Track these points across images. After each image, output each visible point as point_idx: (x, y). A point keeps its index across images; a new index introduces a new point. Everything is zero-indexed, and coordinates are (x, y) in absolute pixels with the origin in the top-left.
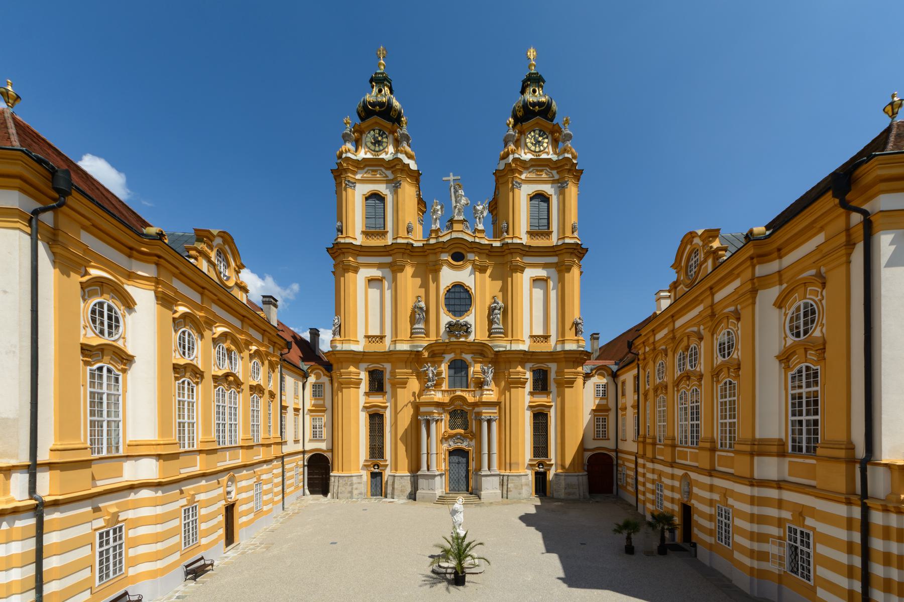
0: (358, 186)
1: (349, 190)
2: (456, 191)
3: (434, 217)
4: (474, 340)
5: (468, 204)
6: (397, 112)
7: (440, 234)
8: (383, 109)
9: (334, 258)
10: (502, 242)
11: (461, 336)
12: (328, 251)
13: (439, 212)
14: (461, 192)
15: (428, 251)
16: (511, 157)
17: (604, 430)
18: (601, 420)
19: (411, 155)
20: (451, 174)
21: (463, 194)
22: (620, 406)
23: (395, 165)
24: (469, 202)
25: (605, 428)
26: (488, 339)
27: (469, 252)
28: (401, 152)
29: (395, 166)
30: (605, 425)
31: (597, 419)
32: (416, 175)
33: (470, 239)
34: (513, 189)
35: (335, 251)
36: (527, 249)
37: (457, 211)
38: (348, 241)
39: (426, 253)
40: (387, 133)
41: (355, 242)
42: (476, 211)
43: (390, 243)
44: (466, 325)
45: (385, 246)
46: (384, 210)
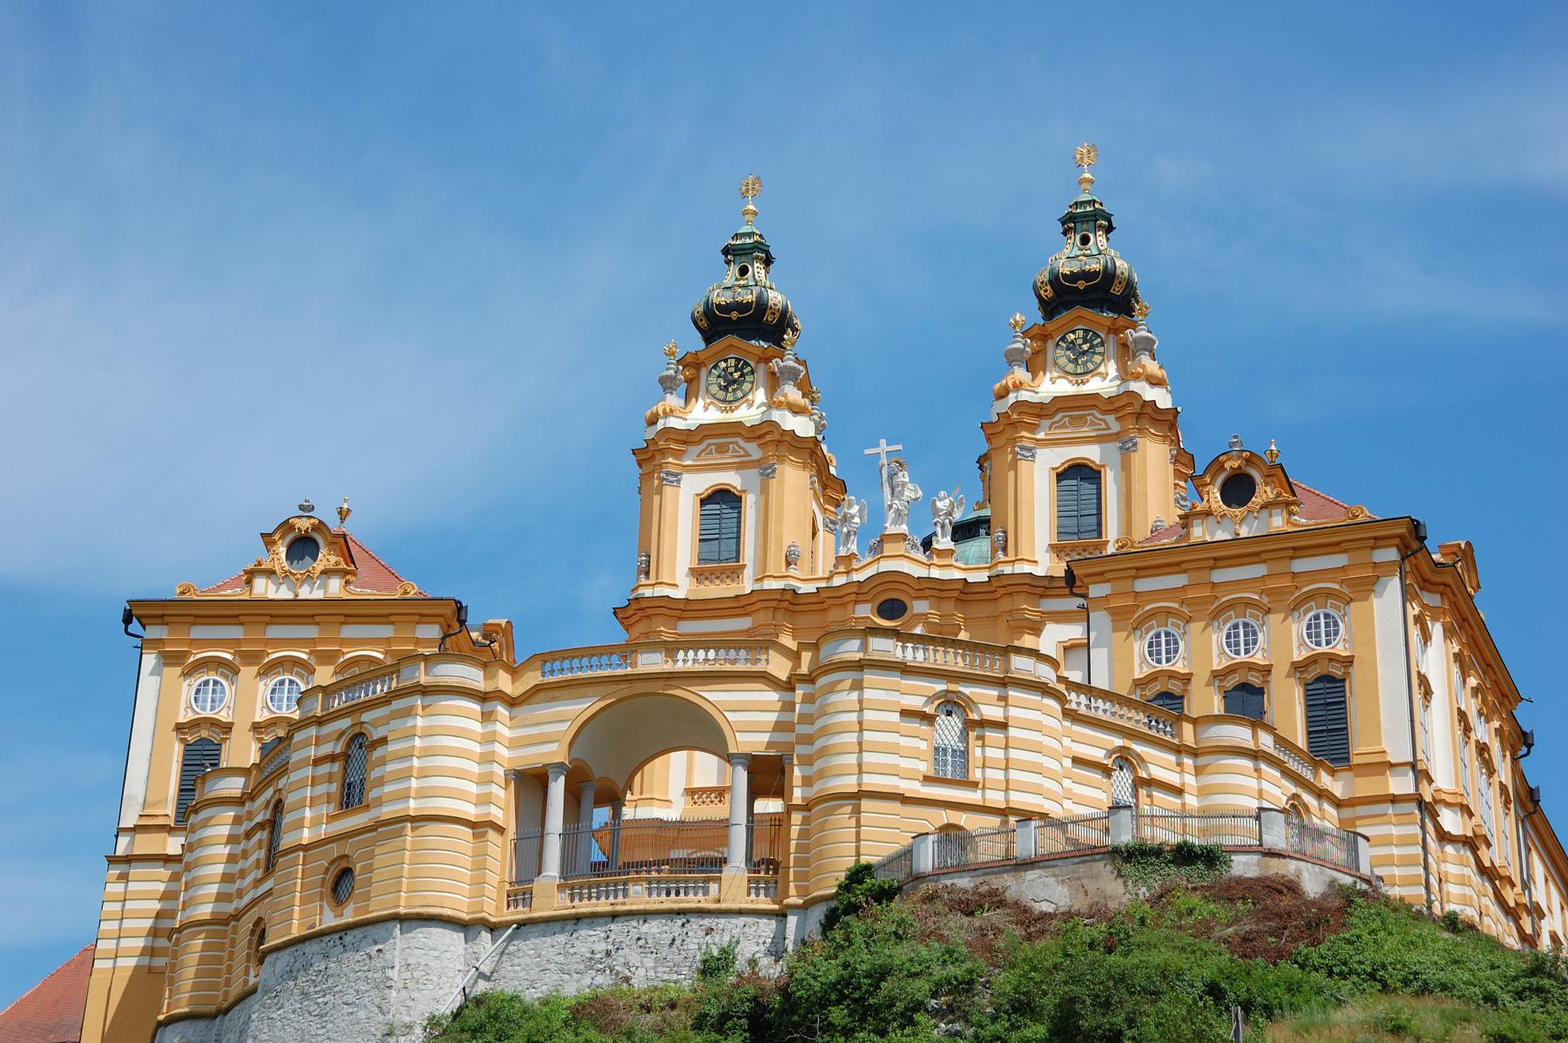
0: (687, 478)
1: (668, 490)
2: (891, 476)
3: (845, 530)
5: (916, 499)
6: (777, 315)
7: (855, 565)
10: (993, 572)
12: (615, 613)
13: (857, 520)
14: (904, 477)
15: (829, 602)
16: (1012, 398)
19: (799, 406)
20: (883, 442)
21: (907, 480)
23: (765, 433)
24: (920, 493)
27: (916, 598)
28: (779, 406)
29: (764, 435)
32: (811, 445)
33: (918, 571)
34: (1014, 465)
35: (632, 612)
36: (1046, 583)
37: (891, 514)
38: (660, 591)
40: (752, 364)
42: (936, 511)
43: (748, 591)
46: (739, 522)
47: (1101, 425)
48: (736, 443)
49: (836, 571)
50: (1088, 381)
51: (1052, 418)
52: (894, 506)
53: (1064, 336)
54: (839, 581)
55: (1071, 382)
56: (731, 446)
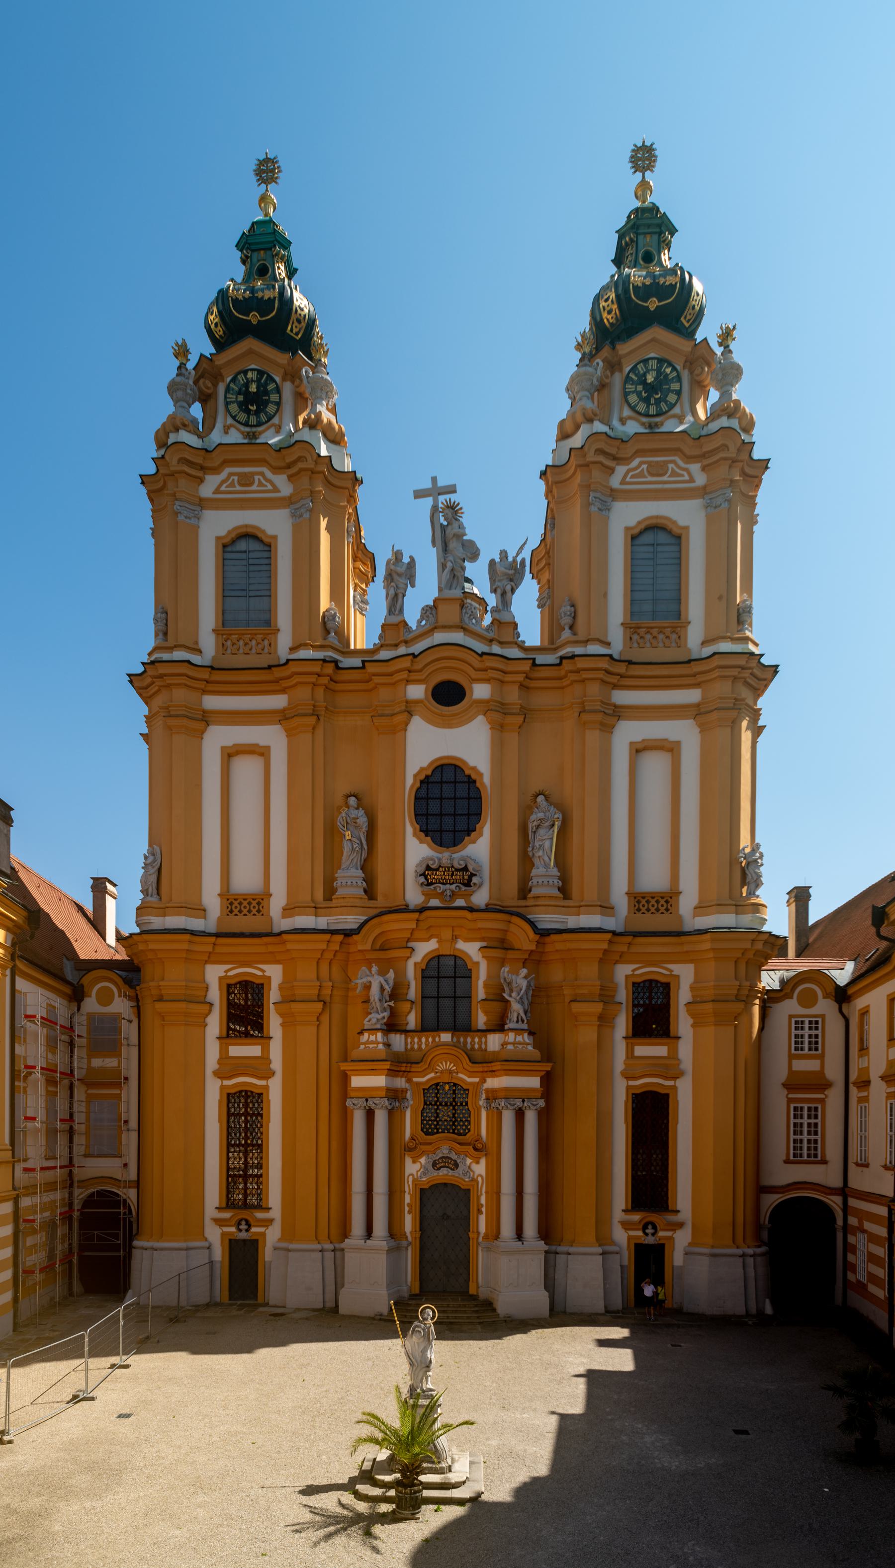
4: (487, 905)
8: (264, 319)
9: (147, 700)
11: (454, 895)
15: (376, 680)
17: (813, 1137)
18: (805, 1113)
22: (853, 1077)
25: (816, 1133)
26: (522, 903)
29: (294, 463)
30: (816, 1125)
31: (795, 1109)
32: (349, 484)
35: (148, 680)
38: (179, 655)
39: (371, 685)
41: (196, 659)
43: (283, 661)
44: (465, 869)
45: (270, 667)
47: (683, 476)
48: (262, 474)
49: (383, 642)
50: (662, 424)
51: (628, 464)
52: (449, 565)
53: (635, 366)
54: (384, 655)
55: (643, 424)
56: (256, 478)
